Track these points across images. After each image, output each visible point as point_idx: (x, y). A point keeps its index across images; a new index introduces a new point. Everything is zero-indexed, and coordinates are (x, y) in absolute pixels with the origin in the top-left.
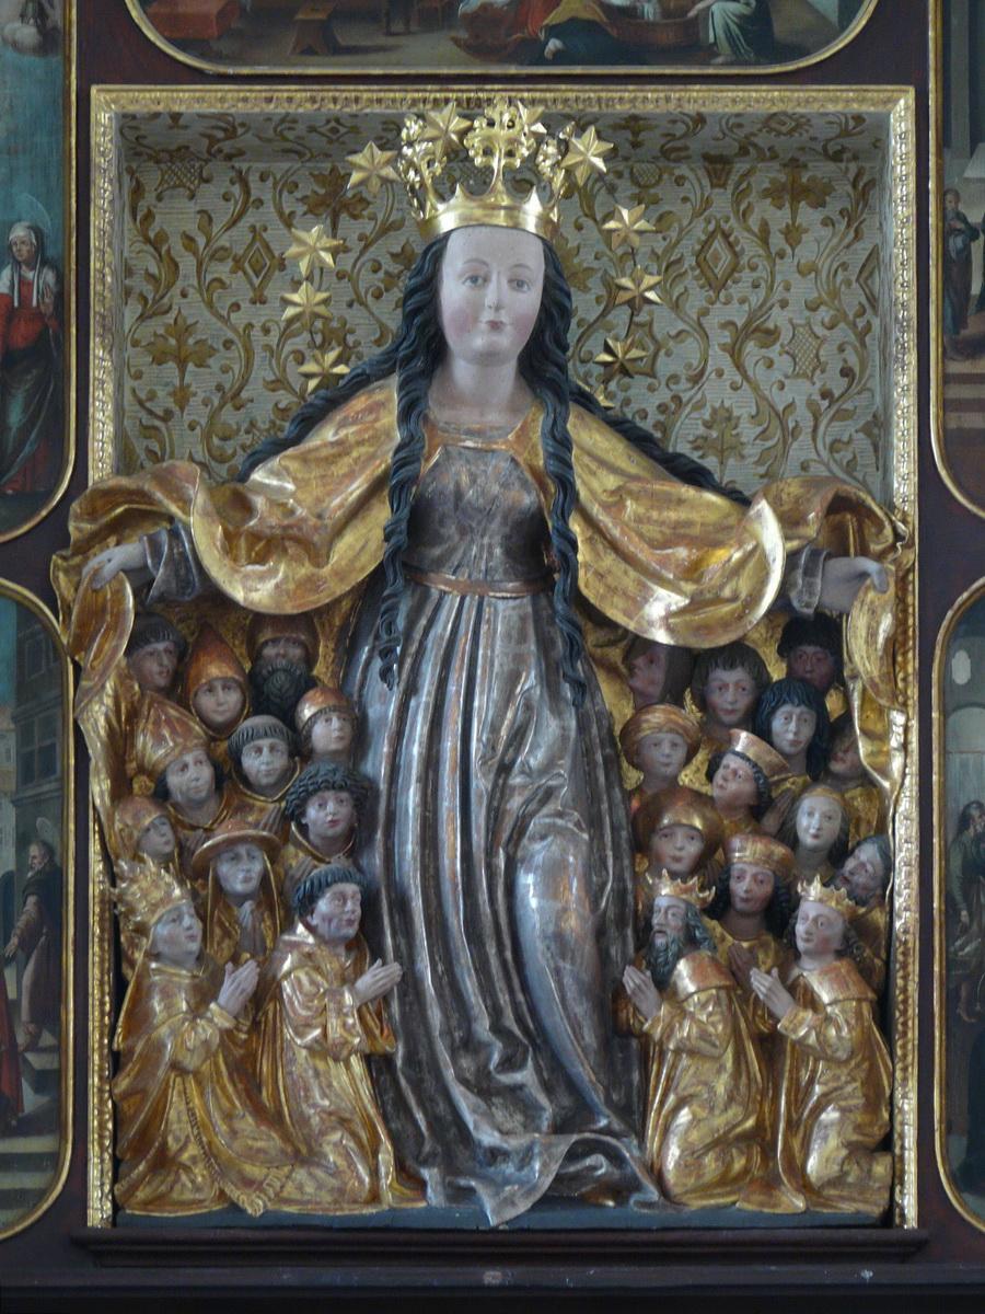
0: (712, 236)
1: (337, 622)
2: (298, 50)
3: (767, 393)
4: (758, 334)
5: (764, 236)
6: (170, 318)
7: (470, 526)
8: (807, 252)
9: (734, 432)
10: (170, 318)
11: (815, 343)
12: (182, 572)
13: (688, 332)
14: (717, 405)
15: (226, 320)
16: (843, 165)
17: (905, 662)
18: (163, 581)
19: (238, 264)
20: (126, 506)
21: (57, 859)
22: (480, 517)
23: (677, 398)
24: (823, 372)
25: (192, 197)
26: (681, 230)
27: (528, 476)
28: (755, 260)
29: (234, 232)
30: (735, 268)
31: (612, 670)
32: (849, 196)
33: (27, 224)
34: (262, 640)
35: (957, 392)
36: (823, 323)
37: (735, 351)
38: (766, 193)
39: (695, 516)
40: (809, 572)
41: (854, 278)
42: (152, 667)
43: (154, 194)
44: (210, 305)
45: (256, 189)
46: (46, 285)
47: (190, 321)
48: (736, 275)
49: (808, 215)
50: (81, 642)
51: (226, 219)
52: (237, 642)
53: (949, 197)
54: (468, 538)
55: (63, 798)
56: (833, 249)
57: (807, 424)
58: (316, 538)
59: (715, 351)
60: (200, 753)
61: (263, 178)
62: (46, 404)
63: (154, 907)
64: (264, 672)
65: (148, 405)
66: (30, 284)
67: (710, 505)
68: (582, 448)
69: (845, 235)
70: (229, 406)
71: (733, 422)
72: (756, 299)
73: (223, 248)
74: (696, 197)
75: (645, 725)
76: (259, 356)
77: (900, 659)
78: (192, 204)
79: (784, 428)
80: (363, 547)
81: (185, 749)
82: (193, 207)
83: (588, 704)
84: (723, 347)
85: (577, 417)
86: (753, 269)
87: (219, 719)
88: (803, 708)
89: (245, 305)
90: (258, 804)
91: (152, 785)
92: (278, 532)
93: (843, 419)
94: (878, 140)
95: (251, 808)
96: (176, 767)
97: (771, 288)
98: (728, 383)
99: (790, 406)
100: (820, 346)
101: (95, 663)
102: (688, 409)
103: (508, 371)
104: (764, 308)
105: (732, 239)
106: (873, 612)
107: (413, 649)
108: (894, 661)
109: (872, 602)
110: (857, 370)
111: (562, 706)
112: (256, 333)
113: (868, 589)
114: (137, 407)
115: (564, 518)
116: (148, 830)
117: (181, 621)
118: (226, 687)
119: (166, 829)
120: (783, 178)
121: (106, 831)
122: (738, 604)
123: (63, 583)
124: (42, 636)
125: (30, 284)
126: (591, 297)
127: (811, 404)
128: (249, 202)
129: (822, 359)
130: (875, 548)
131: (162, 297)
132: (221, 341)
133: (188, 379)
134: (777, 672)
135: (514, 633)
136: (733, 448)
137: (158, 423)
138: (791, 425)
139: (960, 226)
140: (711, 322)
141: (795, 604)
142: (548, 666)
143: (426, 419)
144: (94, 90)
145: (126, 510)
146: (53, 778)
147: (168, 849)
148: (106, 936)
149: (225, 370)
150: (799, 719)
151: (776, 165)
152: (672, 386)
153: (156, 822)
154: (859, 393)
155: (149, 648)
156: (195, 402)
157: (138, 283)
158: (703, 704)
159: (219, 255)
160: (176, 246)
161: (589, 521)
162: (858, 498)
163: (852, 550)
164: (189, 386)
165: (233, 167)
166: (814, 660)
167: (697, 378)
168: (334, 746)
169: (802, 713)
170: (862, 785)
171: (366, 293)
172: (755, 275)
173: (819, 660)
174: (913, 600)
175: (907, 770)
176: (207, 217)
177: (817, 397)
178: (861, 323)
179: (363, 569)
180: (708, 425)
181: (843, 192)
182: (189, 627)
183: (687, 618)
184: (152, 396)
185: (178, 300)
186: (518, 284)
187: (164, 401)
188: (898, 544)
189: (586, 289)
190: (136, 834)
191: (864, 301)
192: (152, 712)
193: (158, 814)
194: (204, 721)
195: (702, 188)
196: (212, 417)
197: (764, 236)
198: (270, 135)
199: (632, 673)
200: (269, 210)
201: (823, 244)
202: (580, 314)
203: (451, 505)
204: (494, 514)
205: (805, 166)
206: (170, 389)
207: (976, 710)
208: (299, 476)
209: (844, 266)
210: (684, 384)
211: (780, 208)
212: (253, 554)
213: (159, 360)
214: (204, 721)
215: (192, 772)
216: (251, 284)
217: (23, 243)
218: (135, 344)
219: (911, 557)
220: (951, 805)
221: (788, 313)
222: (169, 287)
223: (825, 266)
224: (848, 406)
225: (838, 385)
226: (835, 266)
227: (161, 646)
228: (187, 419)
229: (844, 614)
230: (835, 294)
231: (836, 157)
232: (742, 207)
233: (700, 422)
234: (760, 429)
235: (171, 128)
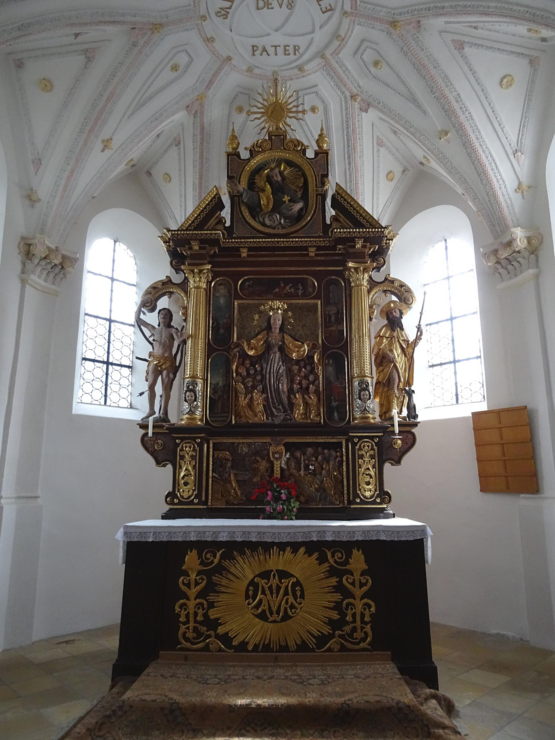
37: (302, 328)
134: (307, 362)
174: (321, 354)
214: (246, 368)
219: (321, 349)
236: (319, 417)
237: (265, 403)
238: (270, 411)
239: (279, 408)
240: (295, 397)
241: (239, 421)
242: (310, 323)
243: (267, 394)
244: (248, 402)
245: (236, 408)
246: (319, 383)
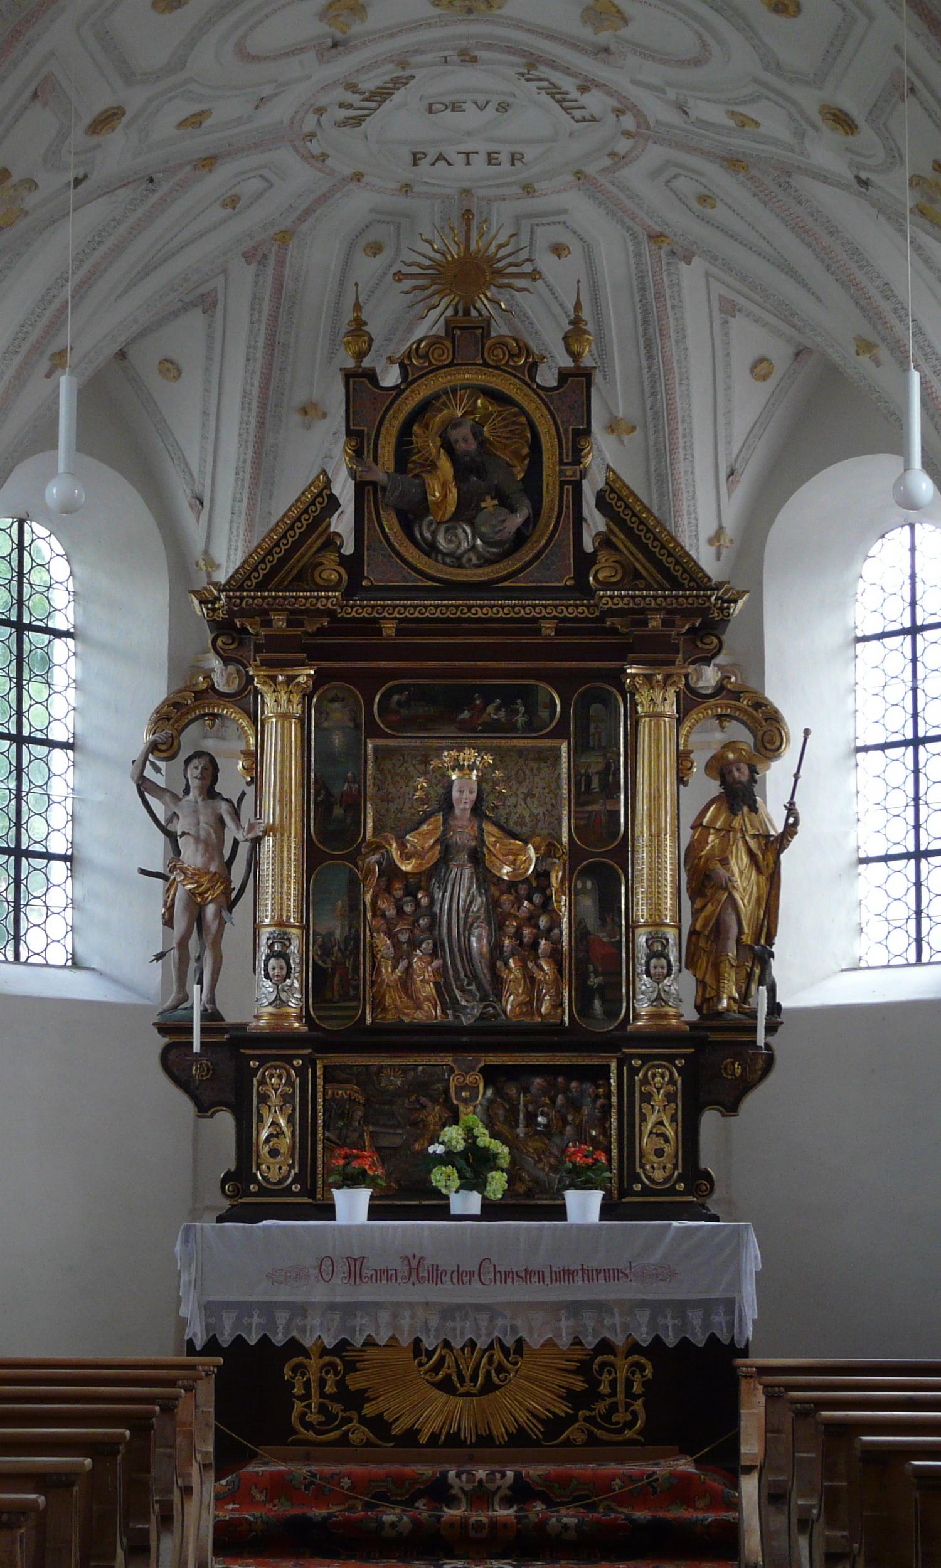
8: (542, 775)
30: (525, 779)
37: (525, 800)
49: (543, 765)
59: (520, 800)
99: (538, 814)
104: (531, 789)
112: (407, 796)
128: (405, 761)
134: (534, 884)
140: (519, 792)
167: (515, 806)
197: (532, 769)
225: (550, 808)
240: (506, 964)
245: (375, 989)
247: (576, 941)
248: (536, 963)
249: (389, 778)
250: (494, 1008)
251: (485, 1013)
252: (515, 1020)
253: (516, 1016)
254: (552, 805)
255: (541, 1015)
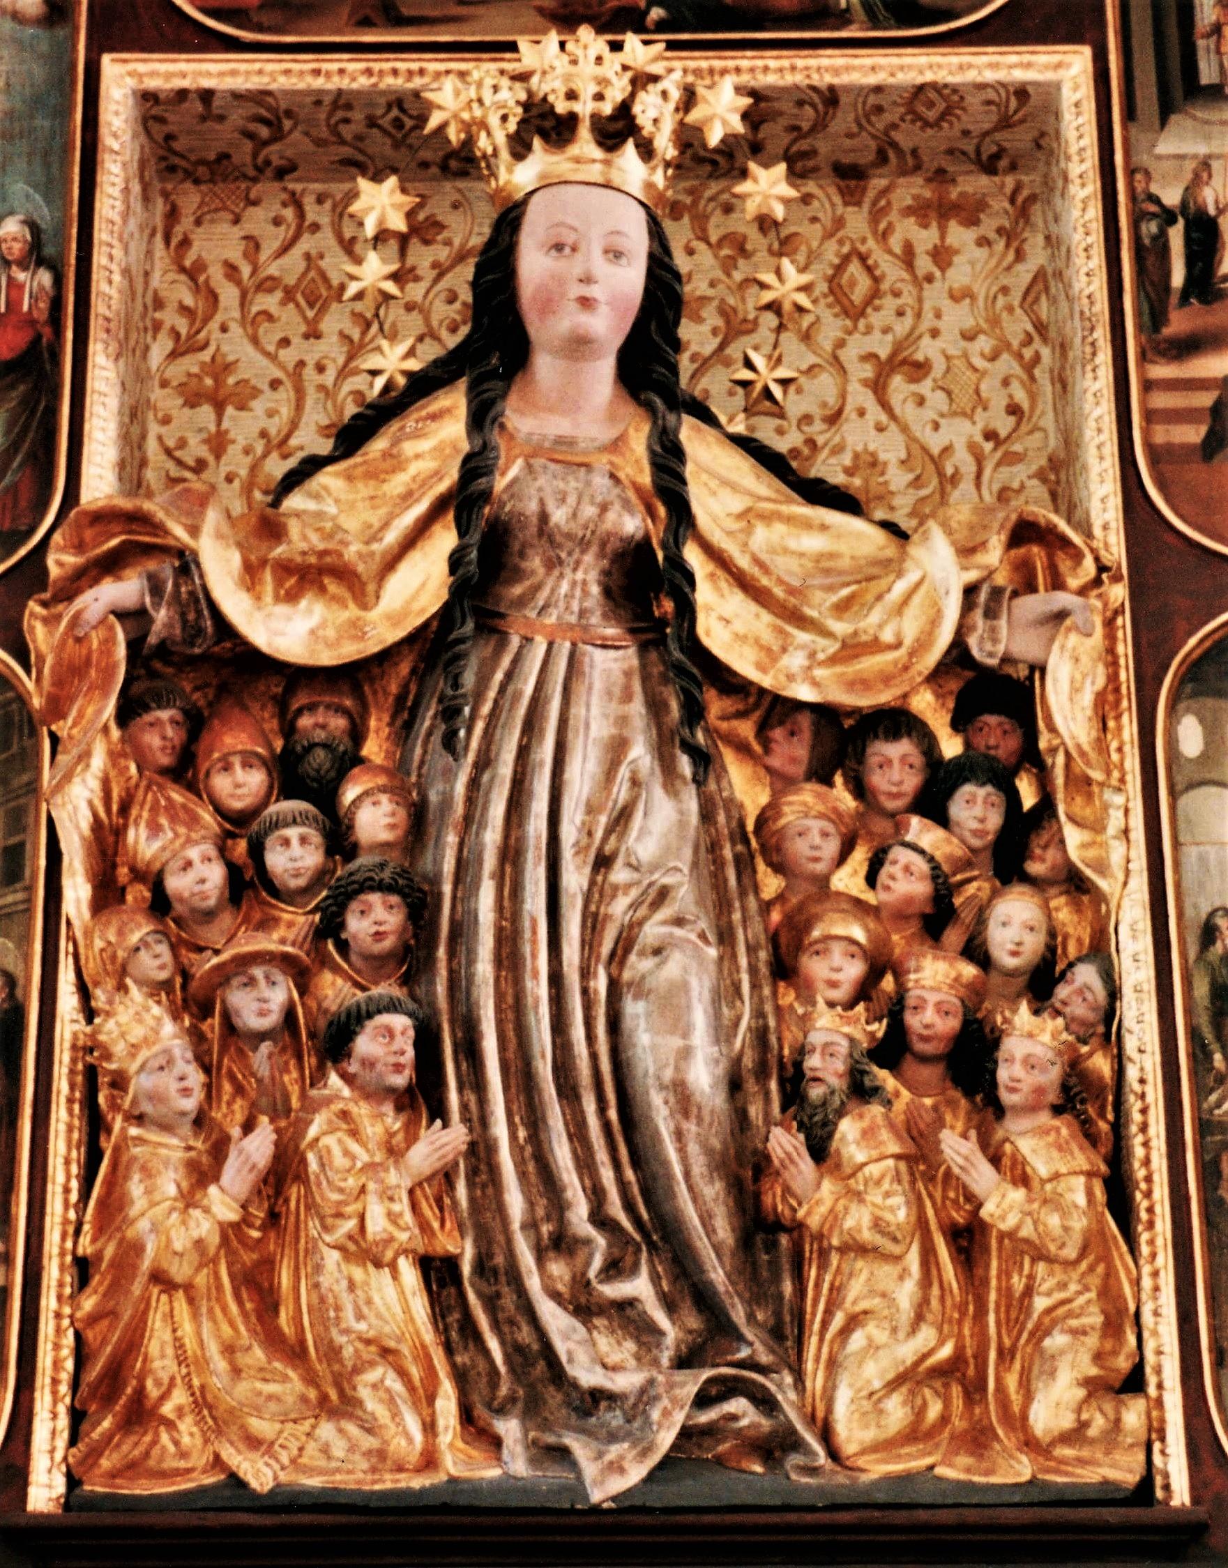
0: (846, 260)
1: (394, 688)
2: (353, 21)
3: (918, 434)
4: (906, 368)
5: (908, 257)
6: (206, 356)
7: (559, 558)
8: (959, 275)
9: (881, 479)
10: (206, 356)
11: (974, 377)
12: (191, 616)
13: (819, 366)
14: (859, 448)
15: (273, 357)
16: (996, 179)
17: (1119, 728)
18: (165, 625)
19: (289, 295)
20: (123, 537)
21: (19, 992)
22: (570, 544)
23: (811, 443)
24: (985, 409)
25: (237, 221)
26: (810, 252)
27: (631, 494)
28: (899, 285)
29: (286, 260)
30: (875, 294)
31: (742, 748)
32: (1007, 212)
33: (21, 217)
34: (295, 706)
35: (1161, 400)
36: (982, 355)
37: (878, 387)
38: (908, 211)
39: (842, 547)
40: (991, 613)
41: (1016, 303)
42: (153, 740)
43: (192, 219)
44: (255, 341)
45: (313, 212)
46: (41, 287)
47: (231, 358)
48: (877, 302)
49: (958, 235)
50: (57, 708)
51: (276, 245)
52: (266, 715)
53: (1138, 177)
54: (556, 572)
55: (29, 911)
56: (992, 271)
57: (969, 467)
58: (361, 568)
59: (854, 387)
60: (209, 849)
61: (320, 200)
62: (35, 424)
63: (134, 1048)
64: (299, 748)
65: (178, 454)
66: (21, 287)
67: (859, 536)
68: (697, 464)
69: (1004, 255)
70: (275, 455)
71: (879, 468)
72: (902, 327)
73: (271, 278)
74: (826, 218)
75: (786, 809)
76: (312, 397)
77: (1111, 724)
78: (236, 229)
79: (940, 473)
80: (423, 585)
81: (189, 842)
82: (237, 232)
83: (712, 786)
84: (865, 383)
85: (692, 428)
86: (897, 294)
87: (238, 805)
88: (989, 788)
89: (296, 340)
90: (286, 916)
91: (147, 894)
92: (313, 560)
93: (1011, 464)
94: (1043, 134)
95: (276, 921)
96: (176, 864)
97: (918, 315)
98: (872, 424)
99: (947, 450)
100: (979, 380)
101: (75, 731)
102: (826, 452)
103: (605, 369)
104: (912, 338)
105: (870, 262)
106: (1077, 660)
107: (486, 709)
108: (1105, 728)
109: (1074, 649)
110: (1026, 406)
111: (678, 783)
112: (309, 373)
113: (1069, 630)
114: (163, 457)
115: (678, 545)
116: (137, 949)
117: (197, 689)
118: (246, 765)
119: (163, 949)
120: (928, 194)
121: (82, 950)
122: (901, 653)
123: (40, 637)
124: (14, 706)
125: (21, 287)
126: (706, 328)
127: (974, 450)
128: (303, 227)
129: (984, 395)
130: (1074, 583)
131: (198, 332)
132: (267, 380)
133: (225, 424)
135: (617, 691)
136: (880, 498)
137: (188, 475)
138: (949, 471)
139: (1153, 208)
140: (850, 355)
141: (975, 652)
142: (660, 735)
143: (502, 427)
144: (106, 59)
145: (123, 543)
146: (18, 886)
147: (163, 975)
148: (77, 1095)
149: (271, 414)
150: (985, 802)
151: (919, 180)
152: (805, 428)
153: (149, 939)
154: (1031, 432)
155: (148, 718)
156: (234, 451)
157: (169, 317)
158: (859, 789)
159: (267, 285)
160: (216, 274)
161: (710, 551)
162: (1049, 522)
163: (1041, 588)
164: (227, 432)
165: (285, 189)
166: (999, 732)
167: (834, 418)
168: (385, 836)
169: (989, 795)
170: (1067, 892)
171: (440, 324)
172: (899, 302)
173: (1005, 732)
174: (1125, 649)
175: (1131, 866)
176: (253, 244)
177: (979, 438)
178: (1028, 353)
179: (423, 611)
180: (849, 472)
181: (998, 213)
182: (205, 696)
183: (839, 669)
184: (182, 443)
185: (216, 334)
186: (615, 254)
187: (196, 449)
188: (1104, 576)
189: (699, 320)
190: (121, 954)
191: (1030, 328)
192: (150, 796)
193: (151, 927)
194: (219, 810)
195: (833, 205)
196: (254, 468)
197: (908, 257)
198: (324, 133)
199: (767, 750)
200: (326, 239)
201: (978, 267)
202: (694, 348)
203: (533, 530)
204: (589, 542)
205: (954, 181)
206: (204, 435)
207: (1213, 790)
208: (343, 497)
209: (1005, 290)
210: (818, 426)
211: (925, 226)
212: (282, 592)
213: (192, 401)
214: (219, 810)
215: (200, 869)
216: (305, 318)
217: (15, 239)
218: (164, 384)
219: (1119, 593)
220: (1189, 912)
221: (939, 343)
222: (207, 320)
223: (981, 290)
224: (1017, 448)
225: (1004, 425)
226: (995, 289)
227: (165, 715)
228: (224, 470)
229: (1039, 668)
230: (995, 322)
231: (989, 167)
232: (882, 226)
233: (839, 469)
234: (911, 476)
235: (204, 119)
236: (1133, 1415)
237: (447, 1243)
238: (515, 1351)
239: (631, 1303)
240: (820, 1150)
241: (132, 1468)
242: (969, 336)
243: (479, 1121)
244: (231, 1233)
245: (89, 1303)
246: (1114, 994)
247: (1194, 1034)
248: (984, 1144)
249: (229, 294)
250: (766, 1403)
251: (709, 1431)
252: (877, 1469)
253: (884, 1447)
254: (1014, 410)
255: (1030, 1444)
